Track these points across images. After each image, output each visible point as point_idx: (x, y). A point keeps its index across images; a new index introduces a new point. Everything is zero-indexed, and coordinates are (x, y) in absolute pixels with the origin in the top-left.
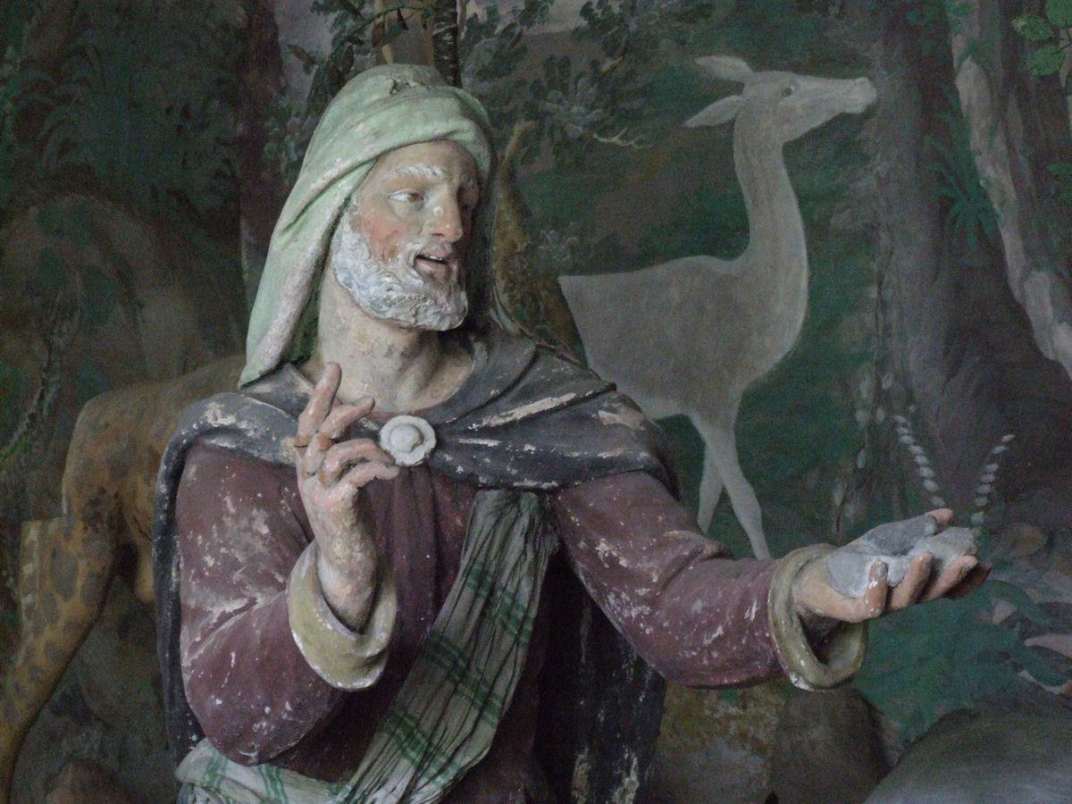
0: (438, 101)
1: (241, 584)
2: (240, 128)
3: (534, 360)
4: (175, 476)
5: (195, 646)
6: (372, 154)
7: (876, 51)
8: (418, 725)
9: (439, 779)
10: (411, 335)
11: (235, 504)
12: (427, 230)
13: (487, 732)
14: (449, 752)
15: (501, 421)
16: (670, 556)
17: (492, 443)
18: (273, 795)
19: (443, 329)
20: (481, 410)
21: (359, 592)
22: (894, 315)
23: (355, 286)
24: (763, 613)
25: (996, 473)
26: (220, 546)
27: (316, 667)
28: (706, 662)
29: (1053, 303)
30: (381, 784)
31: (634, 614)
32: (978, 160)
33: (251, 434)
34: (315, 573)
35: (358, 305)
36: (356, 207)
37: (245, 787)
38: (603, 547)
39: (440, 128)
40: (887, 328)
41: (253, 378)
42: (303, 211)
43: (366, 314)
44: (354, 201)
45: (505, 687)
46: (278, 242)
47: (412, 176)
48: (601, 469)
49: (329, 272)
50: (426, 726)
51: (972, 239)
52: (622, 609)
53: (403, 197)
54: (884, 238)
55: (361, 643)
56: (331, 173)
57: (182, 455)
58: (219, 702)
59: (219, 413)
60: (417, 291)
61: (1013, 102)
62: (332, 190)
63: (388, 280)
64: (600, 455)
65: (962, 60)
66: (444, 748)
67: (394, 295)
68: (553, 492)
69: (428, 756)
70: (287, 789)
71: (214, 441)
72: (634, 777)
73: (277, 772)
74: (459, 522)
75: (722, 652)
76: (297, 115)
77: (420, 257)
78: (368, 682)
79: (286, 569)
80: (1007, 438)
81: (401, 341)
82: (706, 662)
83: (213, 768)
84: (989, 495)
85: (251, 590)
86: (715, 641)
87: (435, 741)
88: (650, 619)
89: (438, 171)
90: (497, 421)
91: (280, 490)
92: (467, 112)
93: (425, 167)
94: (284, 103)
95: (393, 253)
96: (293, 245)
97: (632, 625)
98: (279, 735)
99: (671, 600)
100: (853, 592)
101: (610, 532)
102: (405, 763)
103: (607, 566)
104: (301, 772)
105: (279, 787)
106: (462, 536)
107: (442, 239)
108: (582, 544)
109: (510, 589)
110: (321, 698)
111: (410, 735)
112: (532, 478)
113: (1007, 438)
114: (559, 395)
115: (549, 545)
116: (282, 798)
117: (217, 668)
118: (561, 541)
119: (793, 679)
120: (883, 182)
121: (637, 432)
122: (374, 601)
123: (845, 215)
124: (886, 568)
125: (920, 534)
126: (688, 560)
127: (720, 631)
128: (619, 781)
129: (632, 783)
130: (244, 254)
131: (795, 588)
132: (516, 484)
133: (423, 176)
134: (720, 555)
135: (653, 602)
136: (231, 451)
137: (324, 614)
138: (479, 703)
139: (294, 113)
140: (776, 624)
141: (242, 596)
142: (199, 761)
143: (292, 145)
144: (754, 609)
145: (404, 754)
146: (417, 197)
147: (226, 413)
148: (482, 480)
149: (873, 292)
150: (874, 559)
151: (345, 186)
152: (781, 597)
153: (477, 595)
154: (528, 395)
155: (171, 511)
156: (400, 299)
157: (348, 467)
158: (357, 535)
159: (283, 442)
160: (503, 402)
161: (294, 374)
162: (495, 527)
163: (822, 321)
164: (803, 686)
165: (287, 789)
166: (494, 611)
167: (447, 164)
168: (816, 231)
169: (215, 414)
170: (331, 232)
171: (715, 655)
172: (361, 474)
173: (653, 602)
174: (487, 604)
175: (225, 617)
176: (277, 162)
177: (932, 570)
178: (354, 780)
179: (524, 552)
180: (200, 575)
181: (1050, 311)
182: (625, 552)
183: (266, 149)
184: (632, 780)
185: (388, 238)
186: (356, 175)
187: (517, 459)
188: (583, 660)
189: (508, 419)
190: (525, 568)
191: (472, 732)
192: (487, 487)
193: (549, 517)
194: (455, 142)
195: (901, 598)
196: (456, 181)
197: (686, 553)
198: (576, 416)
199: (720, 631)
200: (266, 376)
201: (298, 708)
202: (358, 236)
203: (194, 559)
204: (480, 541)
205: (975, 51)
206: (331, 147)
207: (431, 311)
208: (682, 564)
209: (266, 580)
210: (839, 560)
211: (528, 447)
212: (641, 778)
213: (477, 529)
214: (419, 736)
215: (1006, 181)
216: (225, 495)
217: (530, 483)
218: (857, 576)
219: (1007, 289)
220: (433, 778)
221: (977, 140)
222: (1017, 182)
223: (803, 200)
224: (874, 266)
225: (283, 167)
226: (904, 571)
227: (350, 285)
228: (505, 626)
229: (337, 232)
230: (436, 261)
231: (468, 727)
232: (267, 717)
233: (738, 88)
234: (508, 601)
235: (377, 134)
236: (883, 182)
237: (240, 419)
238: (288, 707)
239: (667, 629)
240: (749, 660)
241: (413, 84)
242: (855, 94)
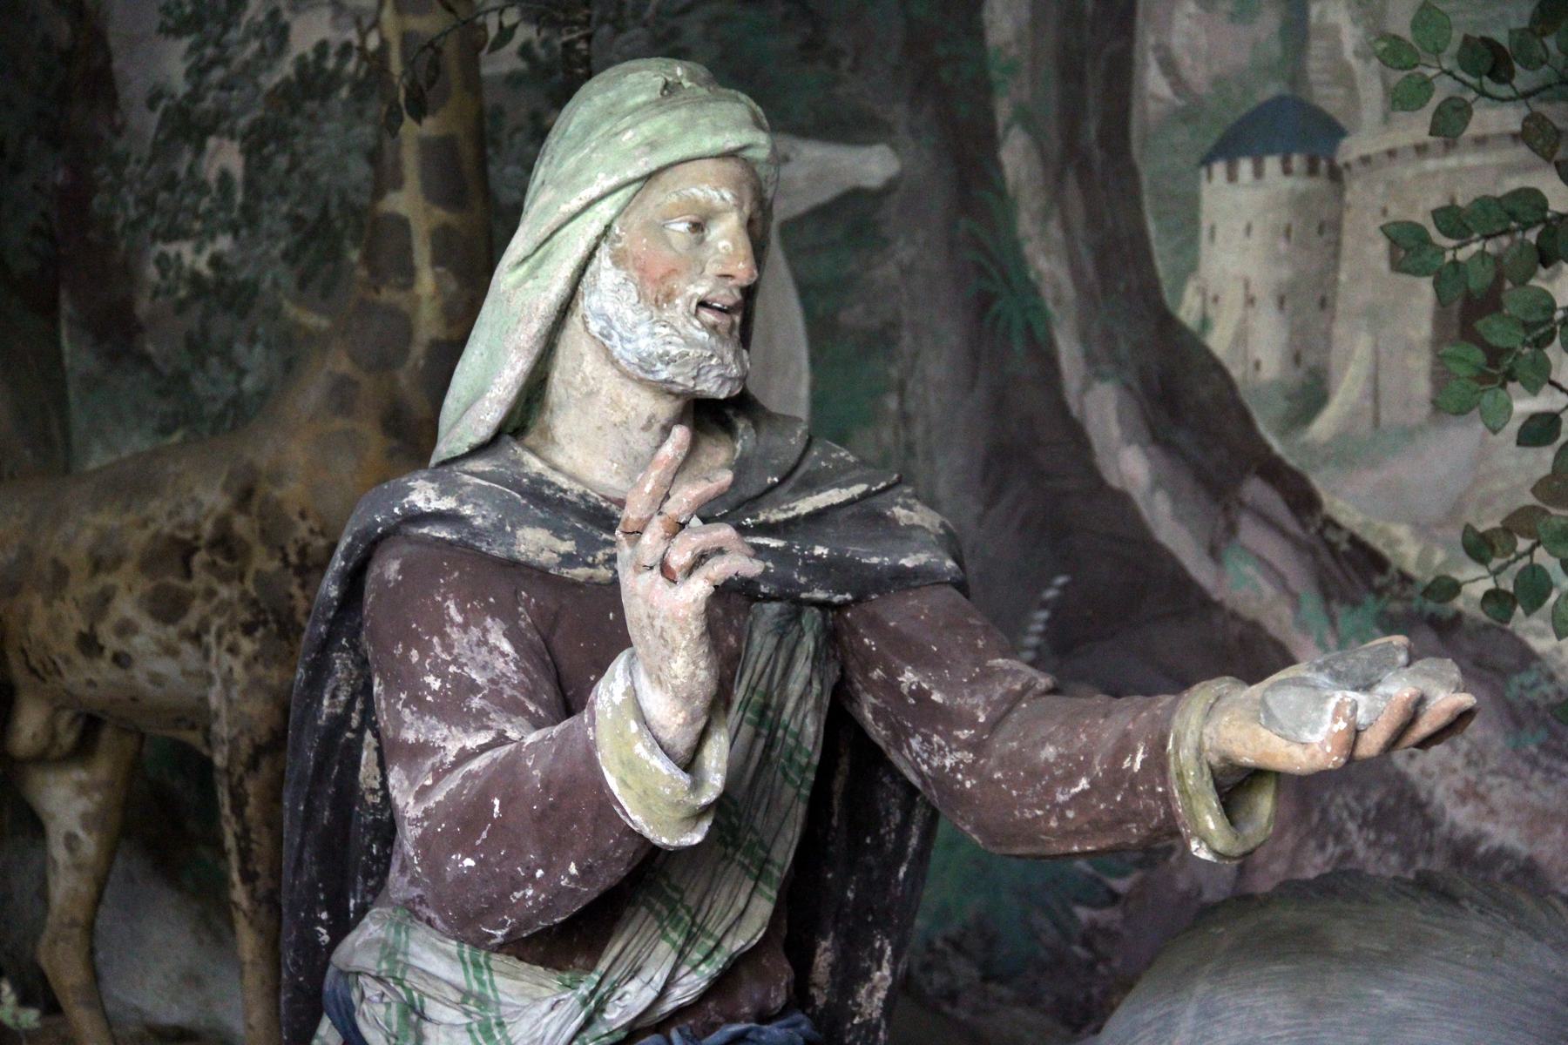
0: (726, 107)
1: (482, 713)
2: (61, 177)
5: (423, 793)
6: (646, 170)
7: (899, 113)
8: (682, 899)
9: (702, 967)
10: (679, 403)
11: (461, 610)
12: (712, 269)
13: (762, 909)
14: (718, 933)
15: (782, 516)
16: (998, 691)
17: (774, 543)
18: (476, 987)
19: (722, 396)
21: (694, 720)
22: (919, 430)
23: (616, 337)
25: (1048, 622)
26: (448, 664)
27: (637, 818)
28: (1053, 824)
29: (1121, 421)
30: (634, 973)
31: (948, 762)
32: (1029, 249)
33: (478, 522)
34: (633, 695)
35: (614, 363)
36: (619, 238)
37: (438, 978)
38: (909, 678)
39: (731, 140)
40: (910, 448)
41: (459, 453)
42: (547, 240)
43: (625, 375)
44: (616, 229)
45: (784, 853)
46: (505, 277)
47: (697, 201)
48: (902, 579)
49: (575, 321)
50: (691, 900)
51: (1018, 344)
53: (683, 227)
54: (907, 340)
55: (696, 786)
56: (593, 191)
57: (371, 546)
58: (469, 862)
59: (432, 495)
60: (703, 347)
61: (1071, 181)
62: (589, 215)
63: (667, 331)
64: (903, 561)
65: (1008, 127)
66: (709, 927)
67: (674, 351)
68: (845, 605)
69: (691, 939)
70: (499, 981)
71: (425, 530)
72: (886, 971)
73: (487, 958)
74: (732, 640)
75: (1081, 811)
76: (138, 161)
77: (703, 304)
78: (696, 838)
80: (1061, 580)
81: (665, 409)
82: (1053, 824)
83: (390, 952)
84: (1037, 649)
85: (499, 721)
86: (1075, 797)
87: (699, 920)
88: (971, 770)
89: (728, 196)
90: (777, 516)
91: (516, 593)
94: (119, 146)
95: (669, 297)
96: (530, 284)
97: (942, 779)
98: (547, 908)
99: (1006, 743)
100: (1307, 736)
101: (921, 660)
102: (664, 946)
103: (912, 701)
104: (521, 959)
105: (486, 977)
107: (731, 282)
108: (877, 673)
109: (793, 727)
110: (620, 859)
111: (673, 911)
112: (826, 589)
113: (1061, 580)
114: (848, 485)
115: (833, 673)
116: (490, 992)
118: (842, 670)
119: (1194, 845)
120: (907, 271)
121: (937, 536)
122: (703, 737)
123: (859, 309)
124: (1355, 709)
125: (1390, 664)
126: (1019, 697)
127: (1084, 783)
128: (866, 976)
129: (883, 978)
130: (64, 332)
131: (1208, 730)
132: (804, 595)
133: (710, 201)
134: (1053, 691)
135: (975, 746)
136: (450, 543)
137: (651, 751)
138: (755, 871)
139: (133, 158)
140: (1180, 775)
141: (488, 728)
142: (368, 945)
143: (131, 199)
144: (1140, 757)
145: (664, 936)
146: (698, 227)
147: (443, 493)
148: (763, 589)
149: (892, 403)
150: (1338, 695)
151: (606, 210)
152: (1190, 740)
153: (757, 735)
154: (811, 484)
156: (683, 355)
157: (700, 559)
158: (704, 648)
159: (519, 533)
160: (782, 492)
161: (519, 450)
162: (778, 648)
164: (1204, 855)
165: (499, 981)
166: (774, 754)
167: (737, 186)
169: (423, 495)
170: (582, 269)
171: (1070, 814)
172: (719, 569)
173: (975, 746)
174: (769, 747)
175: (465, 756)
176: (110, 219)
177: (1418, 705)
178: (603, 966)
179: (810, 683)
180: (416, 701)
181: (1115, 431)
182: (940, 685)
183: (96, 201)
184: (883, 975)
185: (663, 278)
186: (621, 196)
187: (806, 565)
188: (835, 822)
189: (791, 514)
190: (811, 702)
191: (742, 913)
192: (768, 598)
193: (834, 640)
194: (745, 160)
195: (1371, 745)
196: (746, 210)
197: (1018, 687)
199: (1084, 783)
200: (477, 451)
201: (586, 872)
202: (623, 274)
203: (405, 680)
204: (759, 667)
205: (1025, 118)
206: (588, 158)
207: (714, 373)
208: (1014, 699)
211: (820, 550)
212: (894, 973)
213: (755, 649)
214: (682, 912)
215: (1063, 275)
216: (445, 599)
217: (820, 595)
218: (1315, 715)
219: (1062, 408)
220: (695, 968)
221: (1025, 224)
222: (1077, 273)
223: (806, 290)
224: (894, 372)
225: (118, 225)
227: (609, 337)
228: (785, 775)
229: (591, 269)
230: (720, 310)
231: (741, 903)
232: (536, 883)
234: (790, 741)
235: (652, 145)
236: (907, 271)
237: (462, 502)
238: (573, 869)
239: (999, 781)
240: (1121, 822)
241: (687, 84)
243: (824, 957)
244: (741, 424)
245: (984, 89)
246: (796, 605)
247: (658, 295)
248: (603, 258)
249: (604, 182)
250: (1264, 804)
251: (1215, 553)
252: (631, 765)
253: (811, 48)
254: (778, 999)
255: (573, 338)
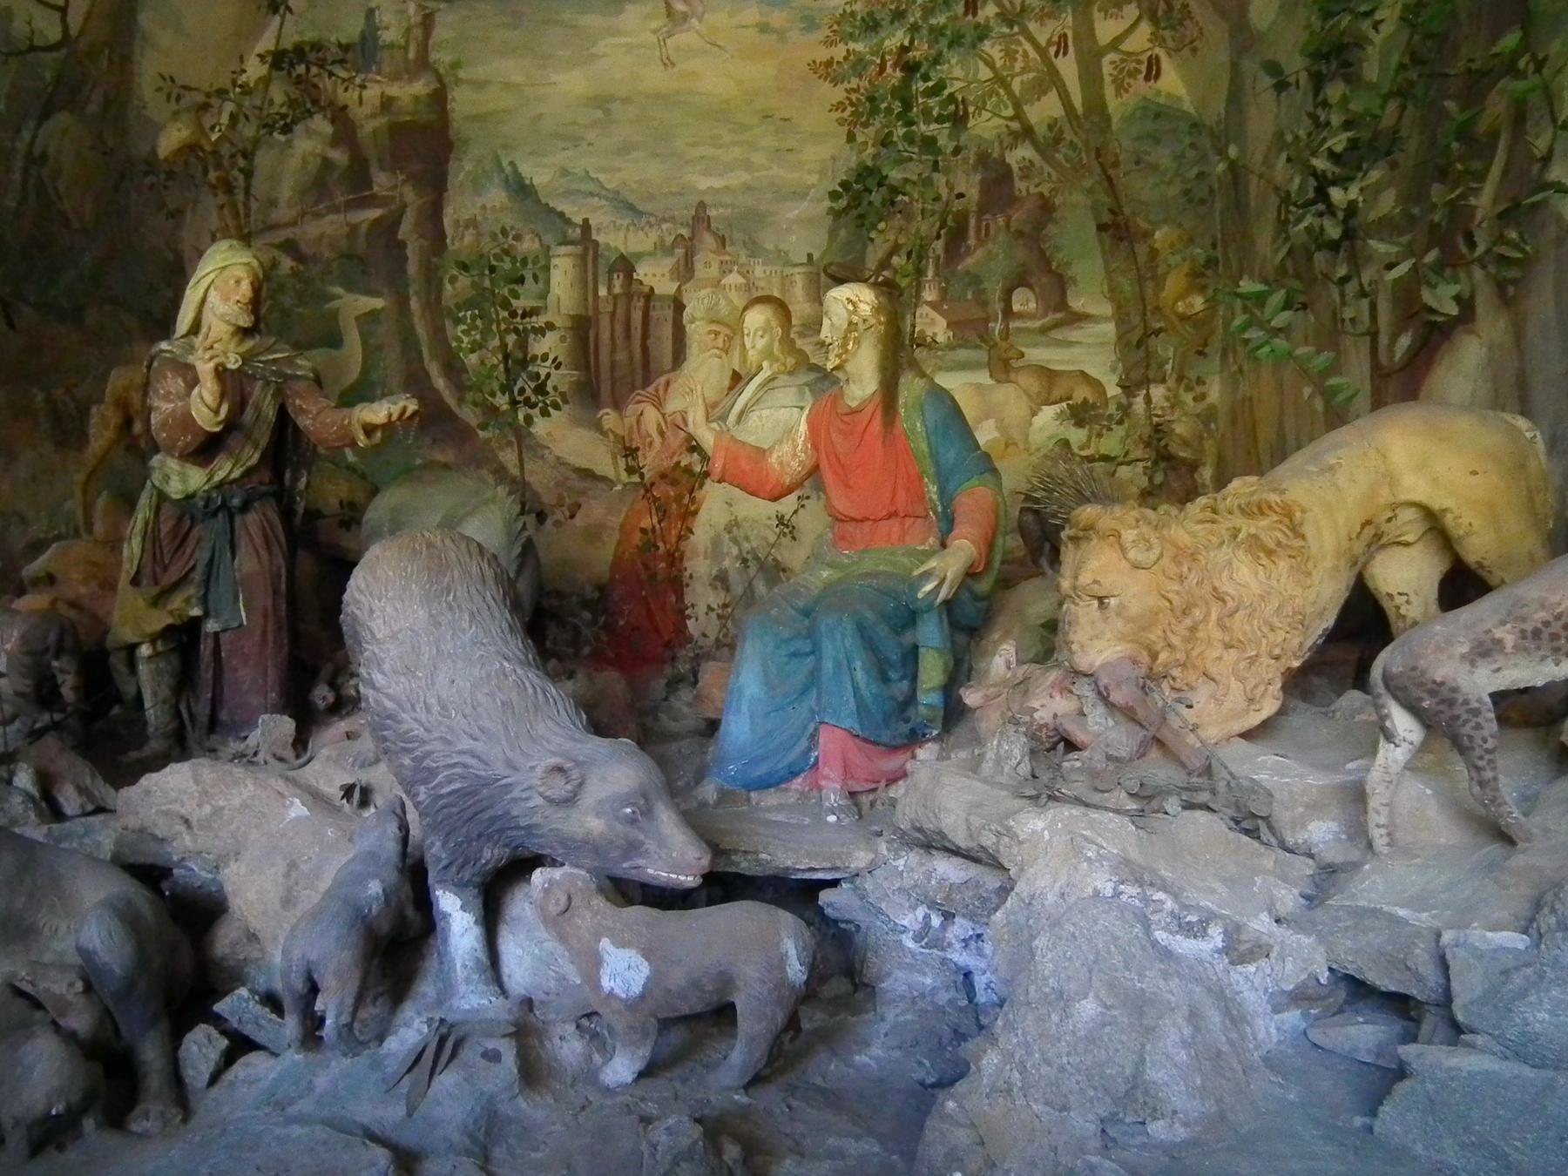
3: (275, 342)
4: (149, 367)
7: (385, 291)
13: (257, 456)
20: (261, 353)
24: (350, 423)
27: (200, 423)
38: (297, 402)
39: (246, 260)
45: (264, 442)
46: (188, 292)
52: (304, 422)
56: (207, 271)
69: (237, 461)
78: (217, 429)
79: (189, 395)
81: (231, 329)
90: (263, 358)
92: (255, 257)
93: (240, 272)
99: (320, 419)
101: (301, 397)
106: (251, 394)
115: (280, 401)
117: (164, 424)
135: (314, 419)
146: (238, 282)
151: (212, 276)
154: (275, 352)
155: (148, 378)
163: (365, 371)
167: (248, 272)
168: (364, 342)
170: (207, 290)
173: (314, 419)
193: (279, 392)
195: (394, 418)
198: (289, 361)
200: (182, 337)
203: (156, 391)
205: (416, 293)
209: (183, 399)
210: (375, 406)
226: (396, 410)
233: (340, 297)
235: (224, 260)
242: (378, 303)
243: (288, 475)
244: (258, 337)
245: (407, 286)
246: (268, 383)
247: (226, 299)
248: (212, 288)
249: (211, 268)
250: (379, 435)
251: (459, 406)
252: (198, 410)
253: (364, 272)
254: (267, 480)
255: (208, 306)
